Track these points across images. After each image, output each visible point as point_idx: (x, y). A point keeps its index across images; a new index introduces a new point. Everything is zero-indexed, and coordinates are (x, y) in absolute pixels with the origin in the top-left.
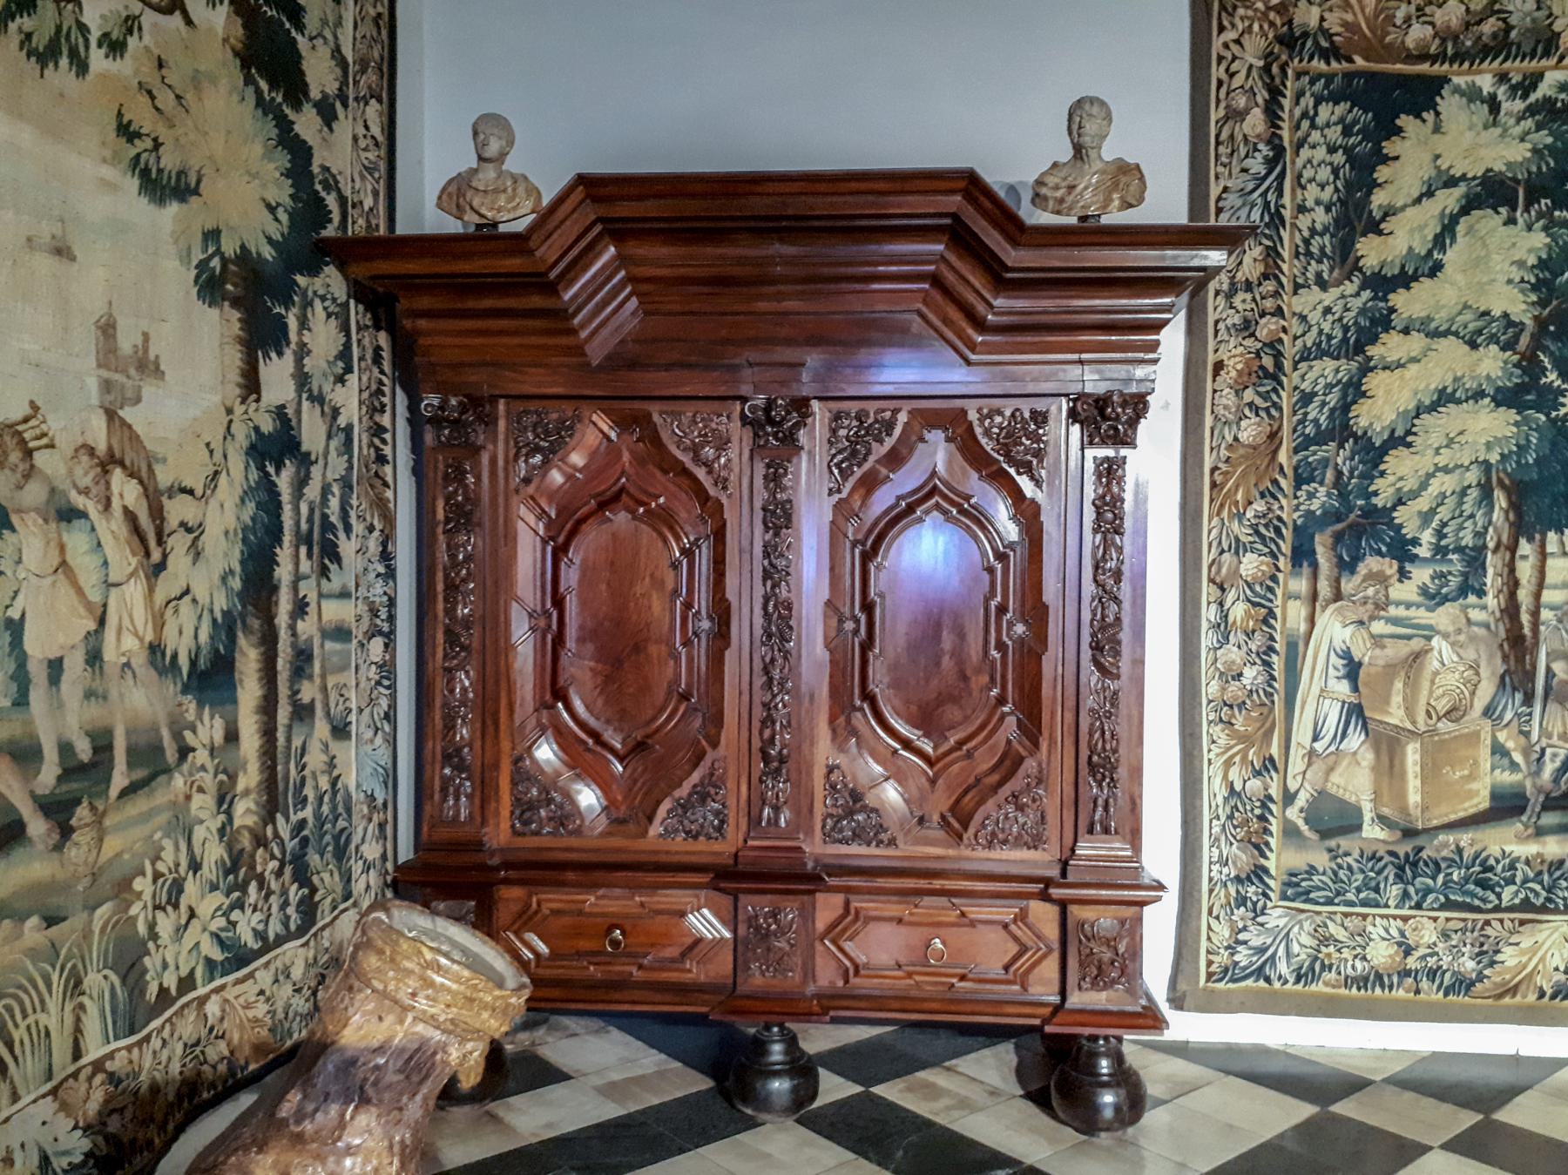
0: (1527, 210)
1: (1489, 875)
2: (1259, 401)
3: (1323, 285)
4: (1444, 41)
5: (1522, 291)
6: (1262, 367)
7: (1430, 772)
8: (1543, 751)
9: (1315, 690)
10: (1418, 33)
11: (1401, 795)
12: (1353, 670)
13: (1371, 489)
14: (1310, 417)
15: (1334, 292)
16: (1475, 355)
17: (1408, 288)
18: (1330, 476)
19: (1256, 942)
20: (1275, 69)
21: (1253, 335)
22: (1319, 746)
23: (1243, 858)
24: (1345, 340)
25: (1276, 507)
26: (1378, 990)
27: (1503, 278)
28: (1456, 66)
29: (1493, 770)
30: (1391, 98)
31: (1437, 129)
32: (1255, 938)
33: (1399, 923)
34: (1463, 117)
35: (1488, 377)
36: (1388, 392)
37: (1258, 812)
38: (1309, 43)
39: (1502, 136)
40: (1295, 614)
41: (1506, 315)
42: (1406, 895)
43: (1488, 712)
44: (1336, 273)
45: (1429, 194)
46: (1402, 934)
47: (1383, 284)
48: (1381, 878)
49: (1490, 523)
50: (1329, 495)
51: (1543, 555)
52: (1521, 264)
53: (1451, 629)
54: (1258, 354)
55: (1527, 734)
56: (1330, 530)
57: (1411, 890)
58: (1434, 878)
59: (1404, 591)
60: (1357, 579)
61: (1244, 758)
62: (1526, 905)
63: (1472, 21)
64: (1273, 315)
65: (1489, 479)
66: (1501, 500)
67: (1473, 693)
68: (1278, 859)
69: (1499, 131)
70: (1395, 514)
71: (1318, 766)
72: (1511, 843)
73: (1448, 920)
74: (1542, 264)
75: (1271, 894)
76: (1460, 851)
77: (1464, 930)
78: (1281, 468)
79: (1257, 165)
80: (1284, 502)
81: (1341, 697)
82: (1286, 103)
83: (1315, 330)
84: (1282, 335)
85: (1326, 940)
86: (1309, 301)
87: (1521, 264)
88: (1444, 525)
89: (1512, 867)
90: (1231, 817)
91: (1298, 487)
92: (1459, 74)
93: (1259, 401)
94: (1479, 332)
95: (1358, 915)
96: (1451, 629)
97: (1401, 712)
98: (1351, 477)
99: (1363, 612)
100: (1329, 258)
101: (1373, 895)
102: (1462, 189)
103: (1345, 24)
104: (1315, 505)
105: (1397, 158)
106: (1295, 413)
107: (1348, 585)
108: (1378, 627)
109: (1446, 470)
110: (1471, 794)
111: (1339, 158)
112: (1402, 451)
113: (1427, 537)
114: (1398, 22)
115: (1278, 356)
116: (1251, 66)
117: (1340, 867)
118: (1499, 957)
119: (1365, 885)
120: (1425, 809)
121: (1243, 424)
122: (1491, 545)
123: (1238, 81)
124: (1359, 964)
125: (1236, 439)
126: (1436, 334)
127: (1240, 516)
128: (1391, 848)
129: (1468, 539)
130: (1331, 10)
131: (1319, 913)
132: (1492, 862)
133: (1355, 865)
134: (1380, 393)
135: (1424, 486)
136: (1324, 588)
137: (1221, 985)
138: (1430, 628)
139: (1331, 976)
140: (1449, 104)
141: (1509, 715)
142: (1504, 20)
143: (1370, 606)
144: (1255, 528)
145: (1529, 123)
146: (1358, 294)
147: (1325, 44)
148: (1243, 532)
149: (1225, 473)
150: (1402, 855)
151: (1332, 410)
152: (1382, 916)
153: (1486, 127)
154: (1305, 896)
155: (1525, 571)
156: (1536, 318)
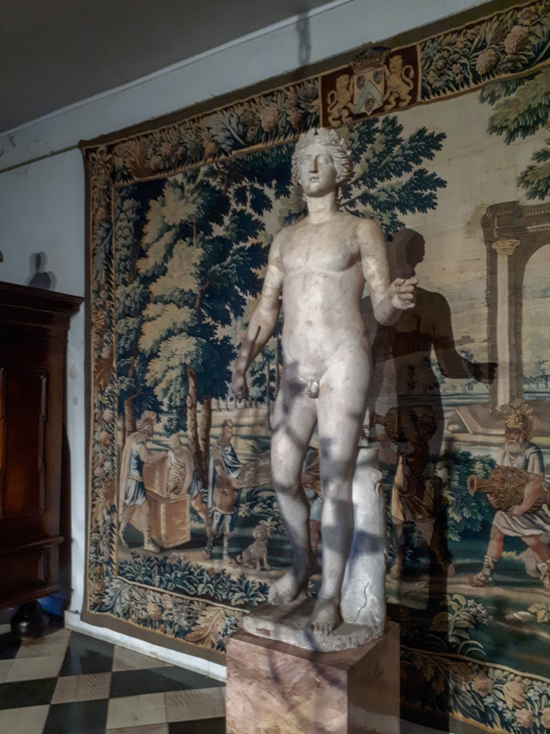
0: (196, 238)
1: (191, 577)
3: (125, 284)
5: (196, 278)
9: (125, 475)
10: (155, 160)
12: (140, 465)
15: (131, 286)
16: (180, 311)
17: (155, 281)
18: (130, 372)
22: (127, 501)
24: (136, 309)
27: (189, 272)
29: (191, 520)
30: (148, 192)
31: (163, 204)
39: (186, 203)
40: (119, 436)
41: (191, 291)
42: (161, 581)
43: (189, 490)
45: (161, 236)
46: (160, 600)
48: (153, 571)
49: (188, 394)
50: (130, 381)
51: (209, 411)
52: (195, 265)
55: (206, 503)
57: (164, 579)
58: (170, 574)
59: (158, 427)
62: (206, 596)
65: (186, 372)
67: (183, 480)
68: (117, 555)
70: (155, 390)
72: (200, 561)
73: (177, 597)
74: (203, 264)
76: (180, 561)
78: (114, 368)
81: (136, 479)
83: (122, 305)
85: (132, 598)
87: (195, 265)
89: (201, 574)
90: (104, 533)
92: (171, 176)
94: (180, 301)
95: (143, 588)
100: (128, 270)
101: (149, 579)
104: (124, 387)
107: (139, 424)
108: (150, 445)
109: (172, 368)
111: (131, 224)
112: (156, 360)
113: (166, 401)
114: (149, 157)
117: (136, 563)
120: (167, 537)
121: (104, 349)
122: (189, 405)
124: (144, 613)
125: (99, 356)
126: (166, 303)
127: (102, 392)
128: (157, 556)
129: (178, 404)
130: (126, 158)
132: (193, 570)
135: (164, 376)
136: (128, 425)
137: (93, 612)
138: (166, 446)
140: (168, 191)
141: (196, 493)
142: (185, 147)
145: (195, 195)
146: (138, 287)
147: (126, 173)
151: (132, 342)
152: (154, 591)
153: (180, 200)
156: (201, 291)
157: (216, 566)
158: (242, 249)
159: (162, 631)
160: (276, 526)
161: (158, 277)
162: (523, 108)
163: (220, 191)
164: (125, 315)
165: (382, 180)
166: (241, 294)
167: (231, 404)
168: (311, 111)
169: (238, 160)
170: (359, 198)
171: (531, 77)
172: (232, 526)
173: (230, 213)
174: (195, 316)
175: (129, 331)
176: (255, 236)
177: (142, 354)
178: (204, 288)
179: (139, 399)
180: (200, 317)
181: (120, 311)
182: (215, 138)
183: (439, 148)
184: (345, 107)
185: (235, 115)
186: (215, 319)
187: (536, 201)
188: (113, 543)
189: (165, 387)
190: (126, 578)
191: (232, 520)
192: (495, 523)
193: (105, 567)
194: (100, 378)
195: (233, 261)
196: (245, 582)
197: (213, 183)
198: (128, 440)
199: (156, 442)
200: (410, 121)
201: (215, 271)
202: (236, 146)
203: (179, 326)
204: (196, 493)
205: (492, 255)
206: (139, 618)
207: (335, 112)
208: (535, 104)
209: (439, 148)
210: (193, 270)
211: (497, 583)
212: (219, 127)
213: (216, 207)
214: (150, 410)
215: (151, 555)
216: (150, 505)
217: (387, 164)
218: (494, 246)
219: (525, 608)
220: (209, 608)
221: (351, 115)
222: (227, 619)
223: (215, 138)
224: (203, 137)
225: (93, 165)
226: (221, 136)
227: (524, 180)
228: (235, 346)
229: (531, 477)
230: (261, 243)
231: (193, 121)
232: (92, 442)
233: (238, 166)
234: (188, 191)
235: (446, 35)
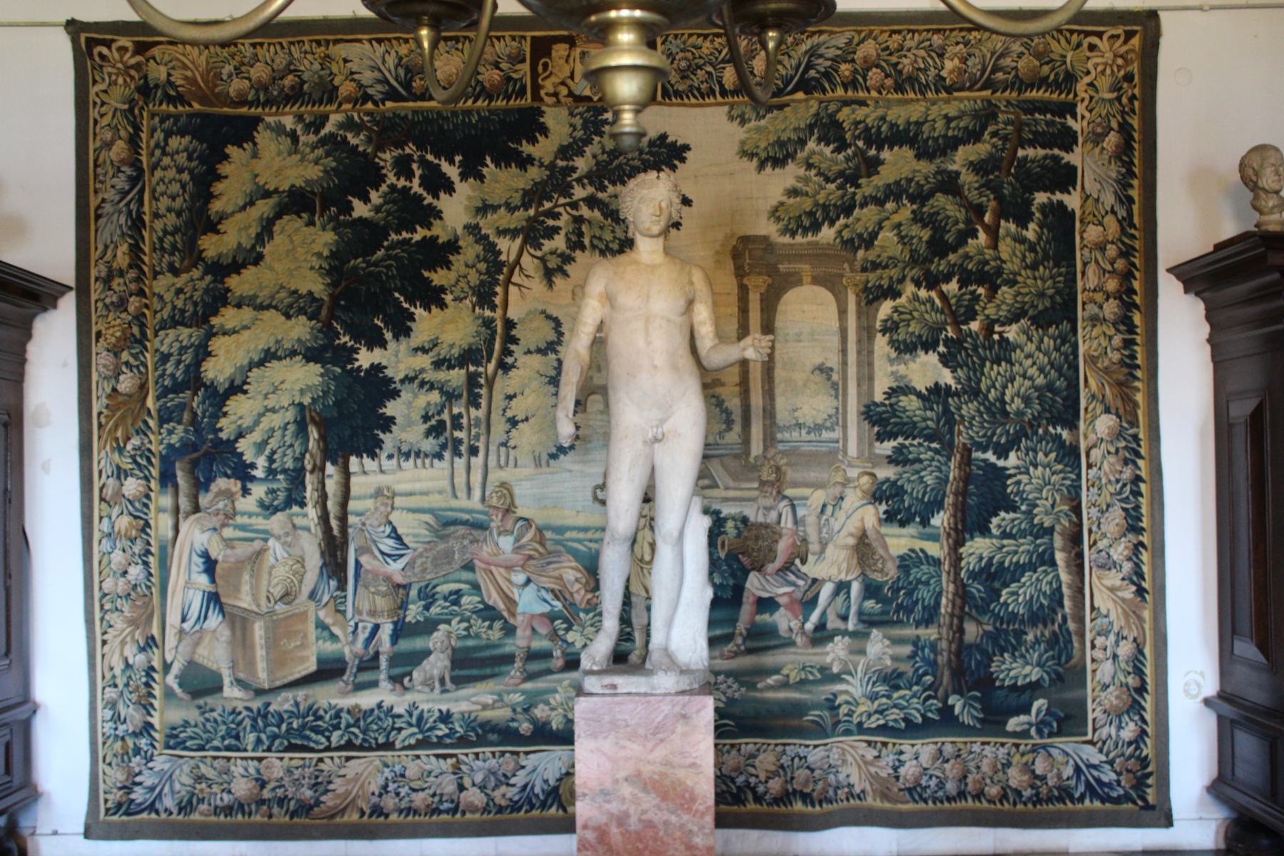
1: (320, 723)
2: (132, 360)
3: (175, 272)
4: (257, 90)
5: (321, 275)
6: (133, 335)
7: (272, 642)
8: (357, 625)
9: (181, 583)
10: (237, 86)
11: (251, 664)
12: (210, 566)
13: (219, 426)
14: (168, 372)
15: (185, 277)
17: (239, 273)
19: (148, 783)
20: (137, 112)
21: (126, 310)
22: (186, 626)
23: (134, 716)
24: (195, 313)
25: (146, 441)
26: (240, 817)
28: (267, 110)
29: (318, 639)
30: (220, 132)
31: (255, 155)
32: (148, 779)
33: (255, 763)
34: (273, 147)
35: (299, 340)
36: (228, 352)
37: (144, 680)
38: (159, 93)
39: (302, 160)
41: (310, 293)
42: (259, 741)
43: (312, 595)
44: (186, 263)
45: (251, 203)
46: (258, 771)
47: (223, 269)
48: (241, 728)
49: (306, 450)
50: (186, 431)
51: (347, 475)
52: (319, 255)
53: (281, 532)
54: (129, 324)
55: (343, 613)
56: (187, 458)
57: (263, 736)
59: (246, 505)
60: (210, 496)
61: (133, 637)
62: (349, 746)
63: (277, 76)
64: (137, 295)
65: (303, 418)
66: (314, 434)
67: (301, 582)
68: (162, 713)
69: (299, 156)
71: (187, 641)
72: (335, 697)
73: (291, 759)
74: (333, 255)
75: (157, 745)
76: (297, 704)
77: (303, 767)
78: (149, 411)
79: (121, 182)
80: (152, 437)
81: (203, 587)
82: (144, 136)
83: (169, 306)
84: (146, 311)
85: (200, 778)
86: (163, 284)
87: (319, 255)
88: (274, 452)
90: (127, 685)
91: (161, 427)
92: (270, 115)
93: (132, 360)
94: (291, 306)
96: (281, 532)
97: (249, 598)
98: (204, 416)
99: (216, 522)
100: (179, 251)
101: (233, 742)
102: (272, 201)
103: (186, 78)
104: (174, 439)
105: (226, 177)
106: (156, 369)
107: (204, 500)
108: (228, 532)
109: (273, 410)
110: (303, 660)
111: (186, 176)
112: (241, 397)
113: (262, 462)
114: (225, 77)
115: (142, 326)
116: (116, 110)
117: (208, 720)
118: (331, 787)
119: (228, 734)
121: (122, 378)
122: (309, 467)
123: (105, 121)
124: (225, 796)
125: (114, 390)
126: (261, 308)
127: (121, 450)
128: (249, 704)
129: (290, 464)
130: (173, 68)
131: (192, 758)
132: (321, 712)
133: (219, 719)
134: (221, 353)
135: (257, 423)
136: (184, 503)
139: (204, 807)
140: (263, 137)
142: (299, 77)
143: (221, 517)
144: (133, 457)
145: (320, 152)
146: (202, 279)
147: (173, 93)
148: (126, 463)
149: (107, 416)
150: (255, 710)
151: (187, 367)
153: (290, 155)
154: (181, 745)
155: (332, 486)
156: (331, 295)
157: (367, 700)
158: (406, 242)
159: (263, 816)
160: (467, 629)
161: (244, 266)
162: (772, 138)
163: (364, 153)
165: (614, 184)
166: (406, 305)
167: (386, 464)
168: (515, 76)
169: (398, 116)
170: (583, 200)
171: (781, 107)
172: (395, 637)
173: (384, 188)
174: (319, 331)
175: (183, 350)
176: (429, 226)
177: (211, 388)
178: (337, 291)
179: (207, 459)
180: (330, 333)
181: (166, 314)
182: (356, 77)
183: (683, 160)
184: (563, 83)
185: (393, 53)
186: (356, 338)
187: (786, 239)
188: (154, 697)
189: (259, 440)
190: (186, 749)
191: (395, 630)
192: (748, 585)
193: (130, 742)
194: (116, 427)
195: (389, 257)
196: (416, 713)
197: (353, 140)
198: (184, 527)
199: (243, 528)
201: (356, 268)
202: (393, 95)
203: (288, 345)
204: (326, 598)
205: (743, 291)
206: (216, 807)
207: (548, 86)
208: (784, 137)
209: (683, 160)
210: (316, 263)
211: (750, 651)
214: (228, 477)
215: (235, 704)
216: (233, 628)
217: (620, 165)
218: (745, 281)
219: (776, 671)
220: (352, 762)
221: (571, 94)
222: (386, 770)
223: (356, 77)
224: (335, 69)
225: (101, 67)
226: (367, 77)
227: (775, 213)
228: (397, 379)
229: (784, 531)
230: (438, 237)
231: (319, 43)
232: (97, 536)
233: (399, 125)
234: (306, 144)
235: (690, 35)
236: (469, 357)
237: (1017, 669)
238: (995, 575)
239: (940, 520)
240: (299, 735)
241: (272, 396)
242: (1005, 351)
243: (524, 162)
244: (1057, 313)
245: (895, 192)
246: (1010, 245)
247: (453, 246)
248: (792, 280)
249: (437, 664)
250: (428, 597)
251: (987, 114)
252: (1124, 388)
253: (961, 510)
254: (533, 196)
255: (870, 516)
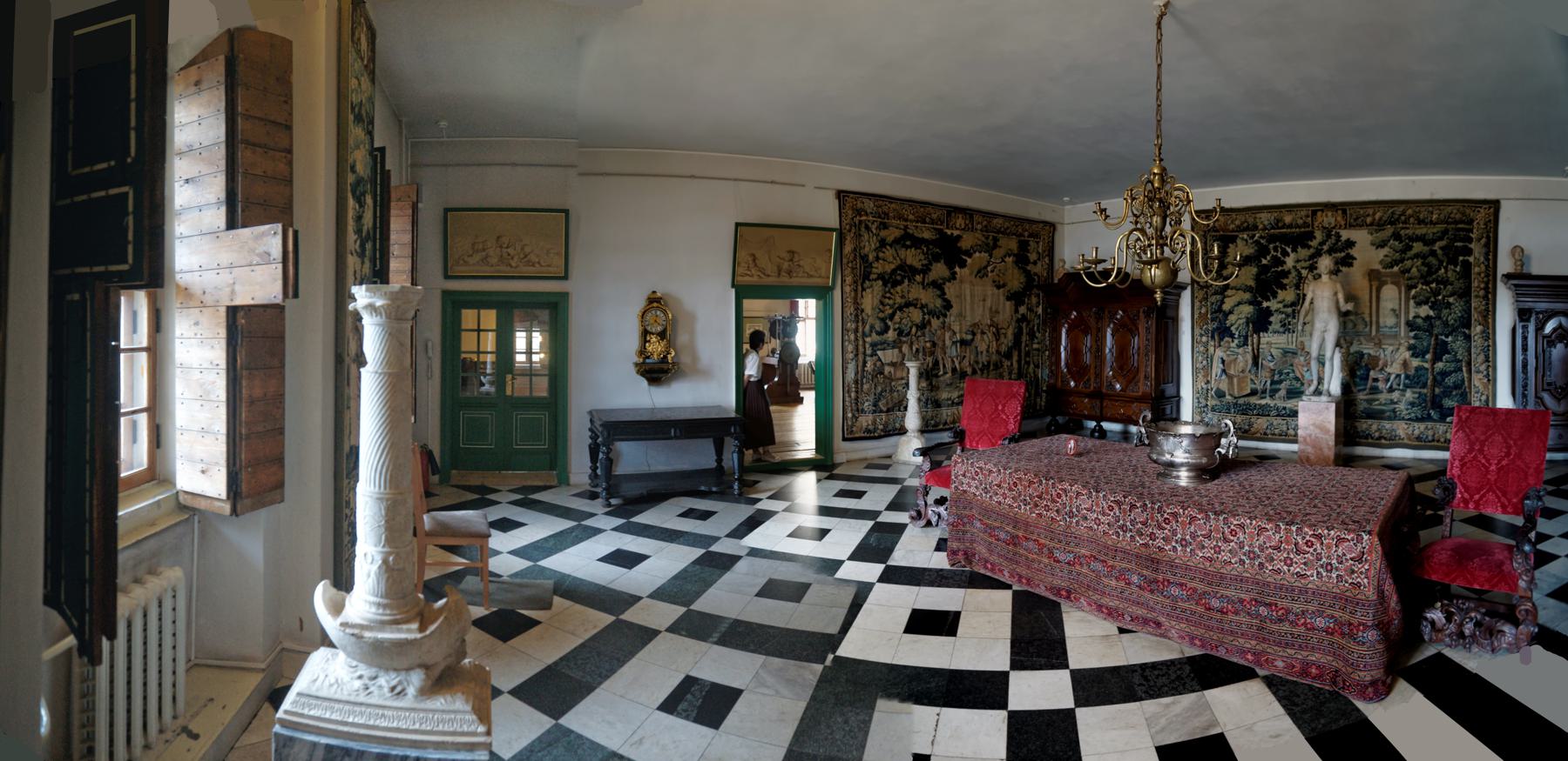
23: (1203, 402)
30: (1227, 241)
157: (1263, 402)
164: (1216, 293)
179: (1223, 332)
200: (1345, 234)
212: (1265, 218)
213: (1262, 251)
236: (1293, 304)
237: (1448, 403)
238: (1444, 374)
239: (1428, 356)
240: (1245, 410)
241: (1239, 315)
242: (1449, 305)
243: (1309, 247)
244: (1465, 294)
245: (1417, 256)
246: (1452, 272)
247: (1289, 272)
248: (1385, 283)
249: (1282, 393)
250: (1280, 373)
251: (1445, 232)
252: (1485, 317)
253: (1435, 353)
254: (1312, 257)
255: (1407, 354)
